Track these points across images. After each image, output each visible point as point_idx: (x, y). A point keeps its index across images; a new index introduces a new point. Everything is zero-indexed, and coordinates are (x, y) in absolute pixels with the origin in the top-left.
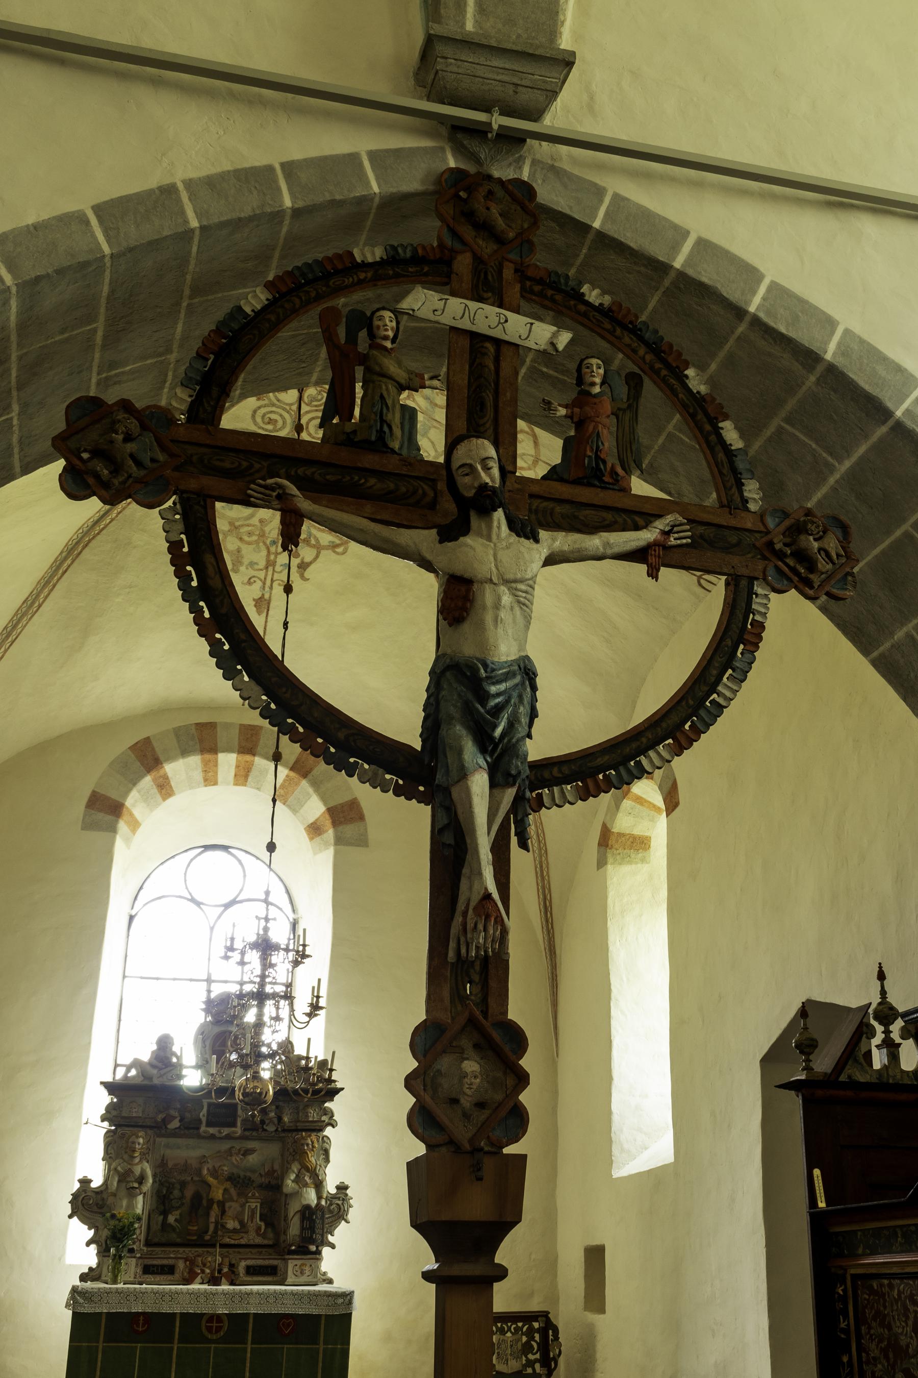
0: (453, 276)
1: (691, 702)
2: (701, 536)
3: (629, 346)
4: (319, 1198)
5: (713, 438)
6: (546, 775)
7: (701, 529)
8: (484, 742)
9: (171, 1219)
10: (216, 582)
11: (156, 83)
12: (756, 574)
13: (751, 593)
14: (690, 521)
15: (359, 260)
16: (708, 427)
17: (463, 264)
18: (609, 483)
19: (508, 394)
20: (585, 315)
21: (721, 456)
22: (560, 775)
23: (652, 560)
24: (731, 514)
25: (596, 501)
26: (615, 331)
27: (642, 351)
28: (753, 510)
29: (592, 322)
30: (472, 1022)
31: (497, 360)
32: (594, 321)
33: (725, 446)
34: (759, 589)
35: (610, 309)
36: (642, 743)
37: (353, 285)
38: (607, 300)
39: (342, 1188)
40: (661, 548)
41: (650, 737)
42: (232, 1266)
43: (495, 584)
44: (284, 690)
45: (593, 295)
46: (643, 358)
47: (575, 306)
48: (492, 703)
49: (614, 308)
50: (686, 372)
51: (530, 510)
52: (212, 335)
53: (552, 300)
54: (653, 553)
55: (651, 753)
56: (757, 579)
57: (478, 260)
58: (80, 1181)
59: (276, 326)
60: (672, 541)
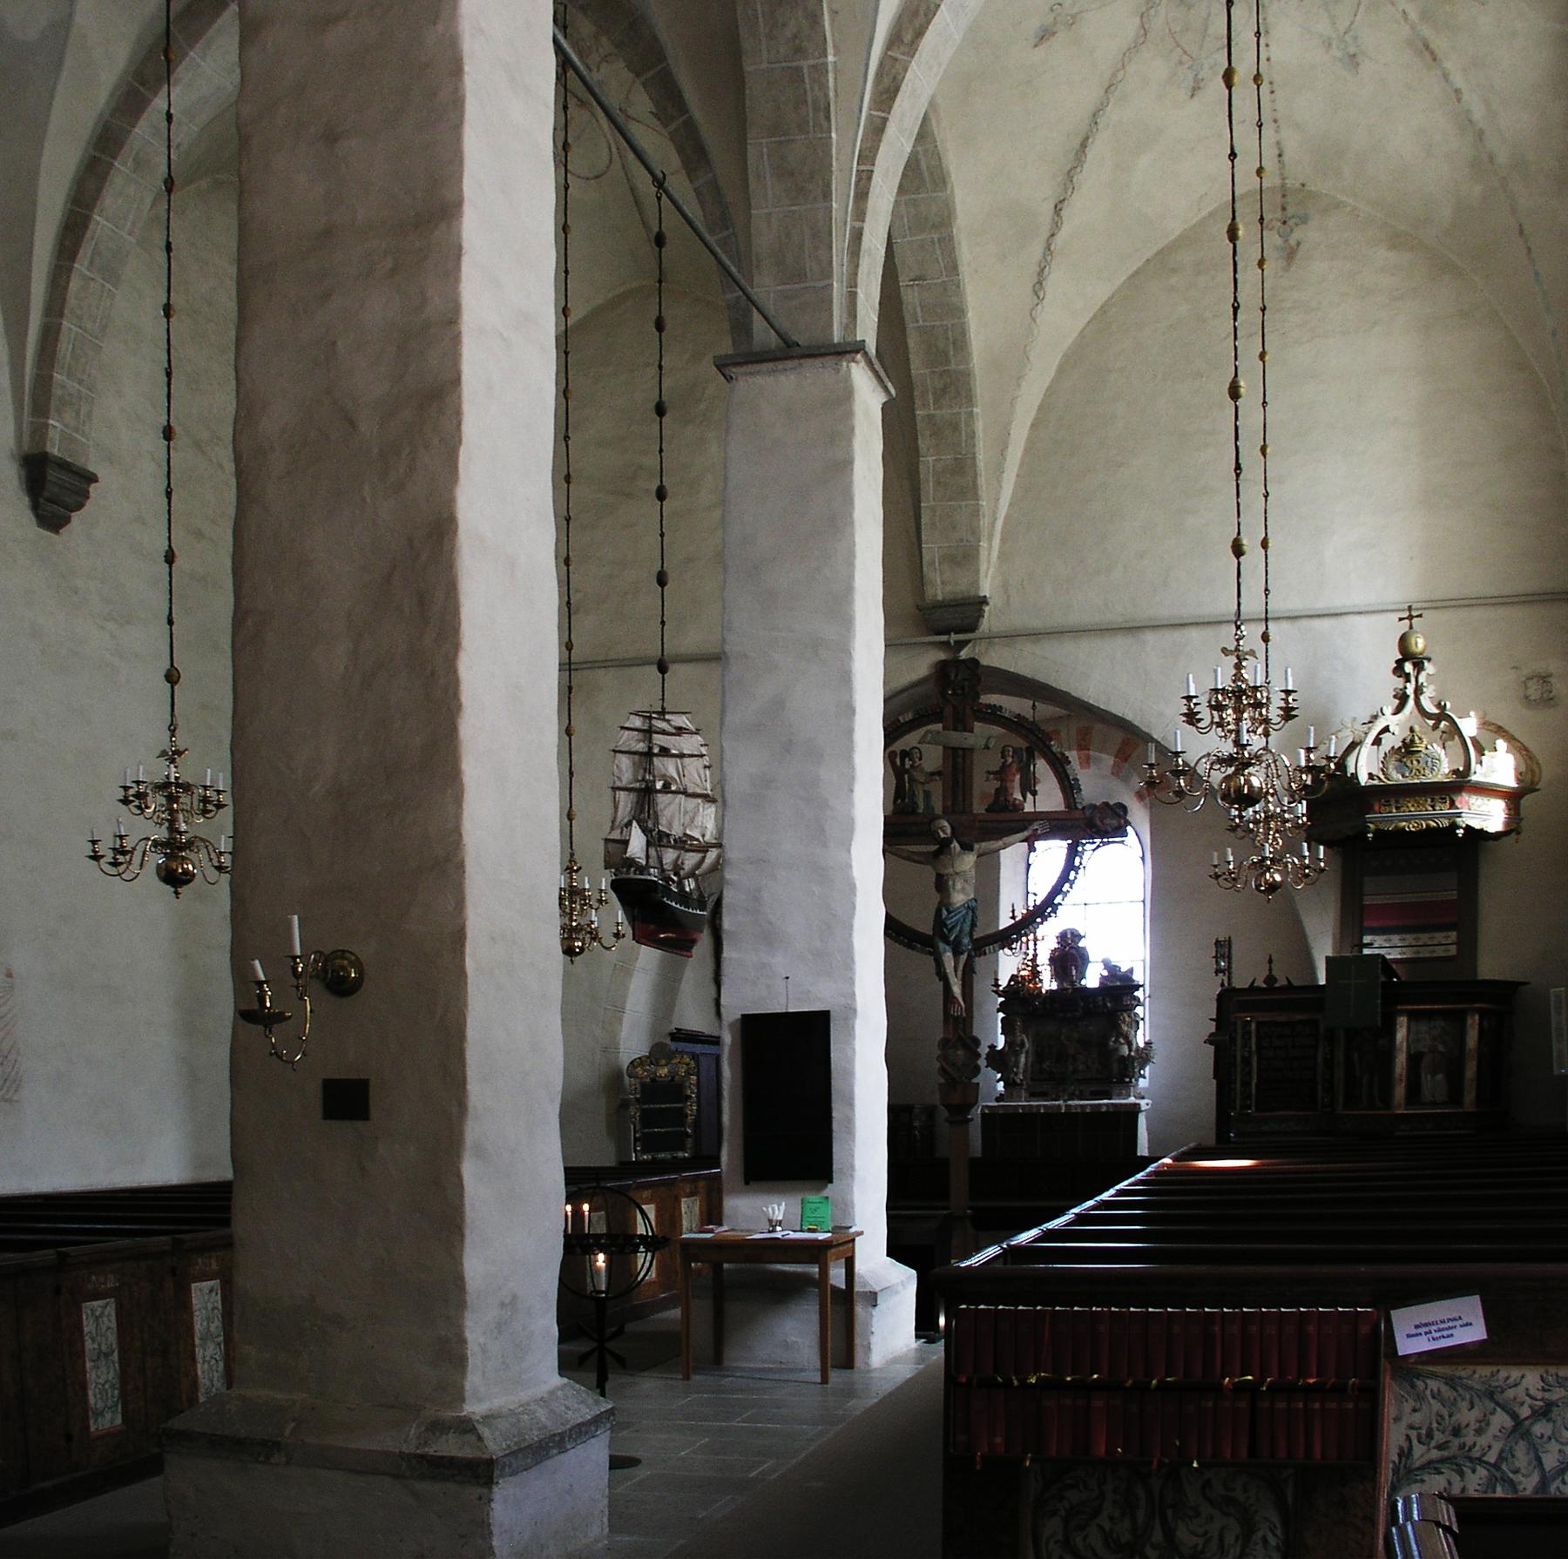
4: (1130, 1050)
5: (1063, 775)
7: (1055, 822)
9: (1044, 1066)
16: (1060, 770)
17: (948, 711)
30: (960, 1038)
31: (964, 758)
39: (1148, 1044)
42: (1081, 1091)
57: (954, 707)
58: (989, 1047)
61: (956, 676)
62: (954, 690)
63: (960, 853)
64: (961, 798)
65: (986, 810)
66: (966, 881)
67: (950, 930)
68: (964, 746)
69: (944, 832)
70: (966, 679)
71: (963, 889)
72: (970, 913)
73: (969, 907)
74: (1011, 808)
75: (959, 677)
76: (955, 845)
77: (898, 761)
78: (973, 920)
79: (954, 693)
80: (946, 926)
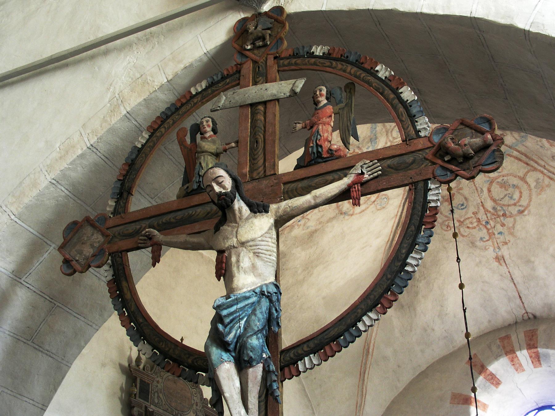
0: (242, 78)
1: (389, 276)
2: (389, 167)
3: (341, 69)
5: (396, 101)
6: (300, 351)
7: (389, 162)
8: (224, 346)
10: (128, 296)
11: (106, 53)
12: (428, 177)
13: (427, 190)
14: (379, 160)
15: (194, 93)
16: (392, 96)
17: (248, 68)
18: (328, 157)
19: (270, 130)
20: (315, 64)
21: (401, 109)
22: (309, 349)
23: (354, 194)
24: (408, 145)
25: (330, 169)
26: (332, 64)
27: (349, 67)
28: (423, 136)
29: (319, 66)
32: (320, 65)
33: (403, 103)
34: (431, 186)
35: (329, 54)
36: (358, 313)
37: (191, 107)
38: (326, 49)
40: (359, 185)
41: (363, 307)
43: (236, 248)
44: (161, 344)
45: (318, 50)
46: (350, 73)
47: (308, 61)
48: (227, 320)
49: (331, 52)
50: (376, 69)
51: (284, 193)
52: (123, 166)
53: (296, 64)
54: (354, 189)
55: (365, 318)
56: (430, 179)
57: (255, 62)
59: (152, 148)
60: (366, 177)
61: (256, 28)
62: (253, 44)
63: (247, 219)
64: (261, 162)
65: (294, 169)
66: (257, 254)
67: (225, 326)
68: (265, 99)
69: (220, 184)
70: (268, 29)
71: (254, 267)
72: (265, 303)
73: (262, 293)
74: (325, 155)
75: (259, 28)
76: (239, 205)
77: (188, 140)
78: (270, 314)
79: (255, 47)
80: (222, 322)
